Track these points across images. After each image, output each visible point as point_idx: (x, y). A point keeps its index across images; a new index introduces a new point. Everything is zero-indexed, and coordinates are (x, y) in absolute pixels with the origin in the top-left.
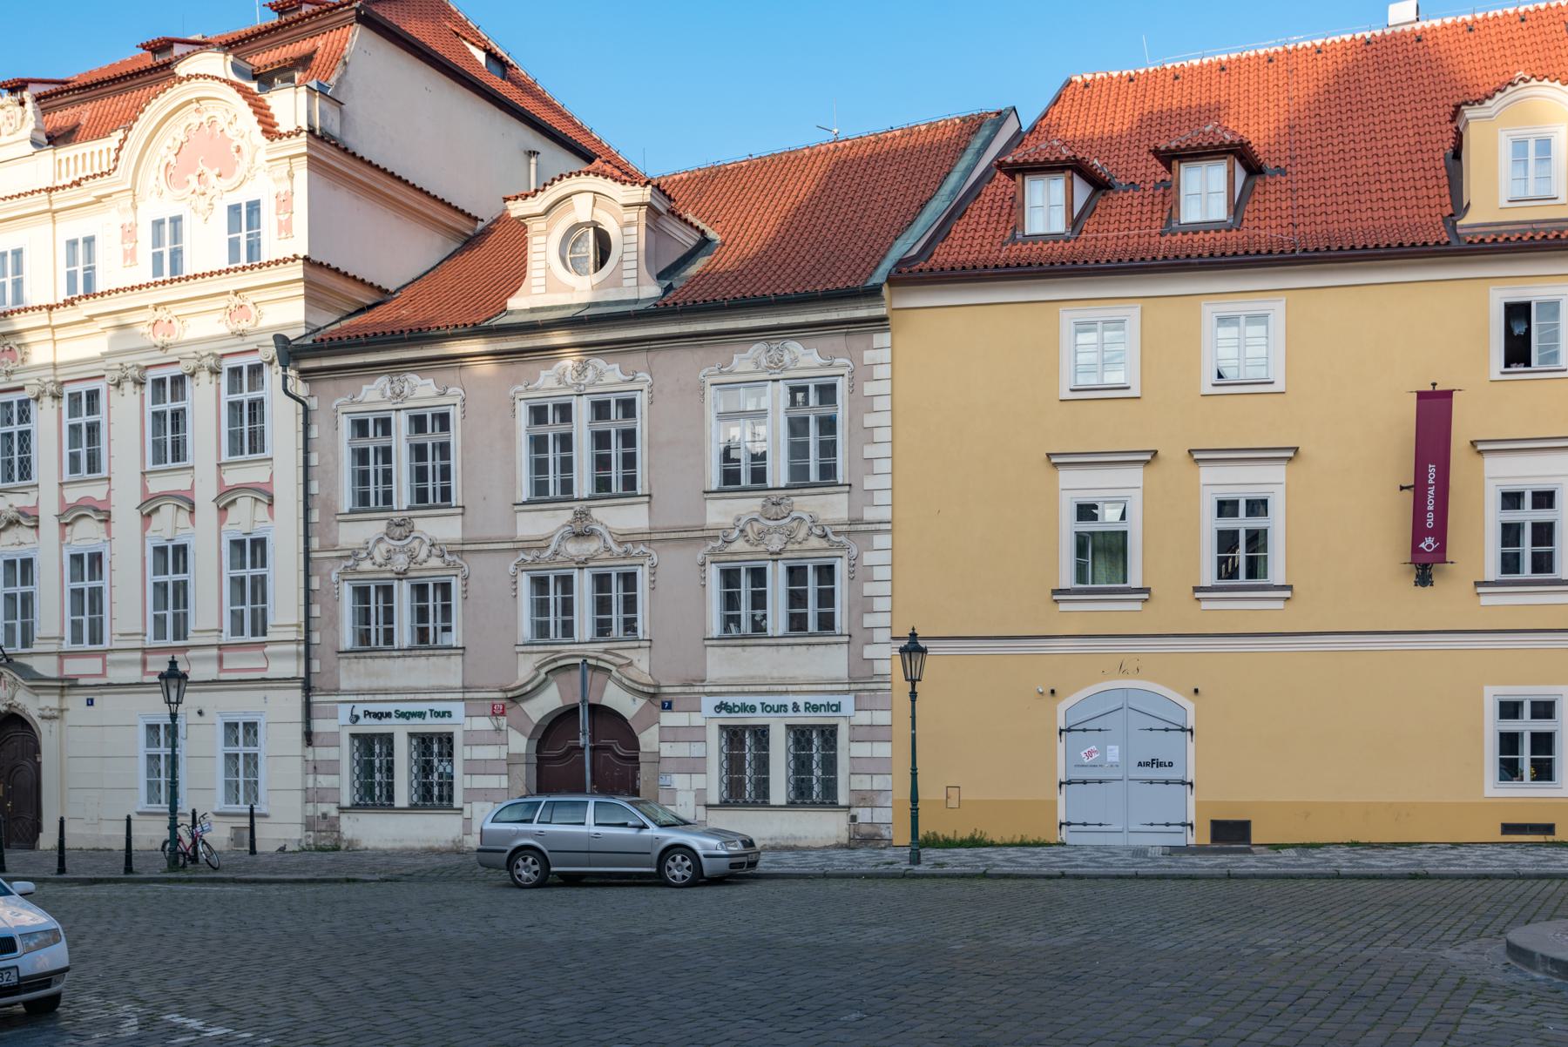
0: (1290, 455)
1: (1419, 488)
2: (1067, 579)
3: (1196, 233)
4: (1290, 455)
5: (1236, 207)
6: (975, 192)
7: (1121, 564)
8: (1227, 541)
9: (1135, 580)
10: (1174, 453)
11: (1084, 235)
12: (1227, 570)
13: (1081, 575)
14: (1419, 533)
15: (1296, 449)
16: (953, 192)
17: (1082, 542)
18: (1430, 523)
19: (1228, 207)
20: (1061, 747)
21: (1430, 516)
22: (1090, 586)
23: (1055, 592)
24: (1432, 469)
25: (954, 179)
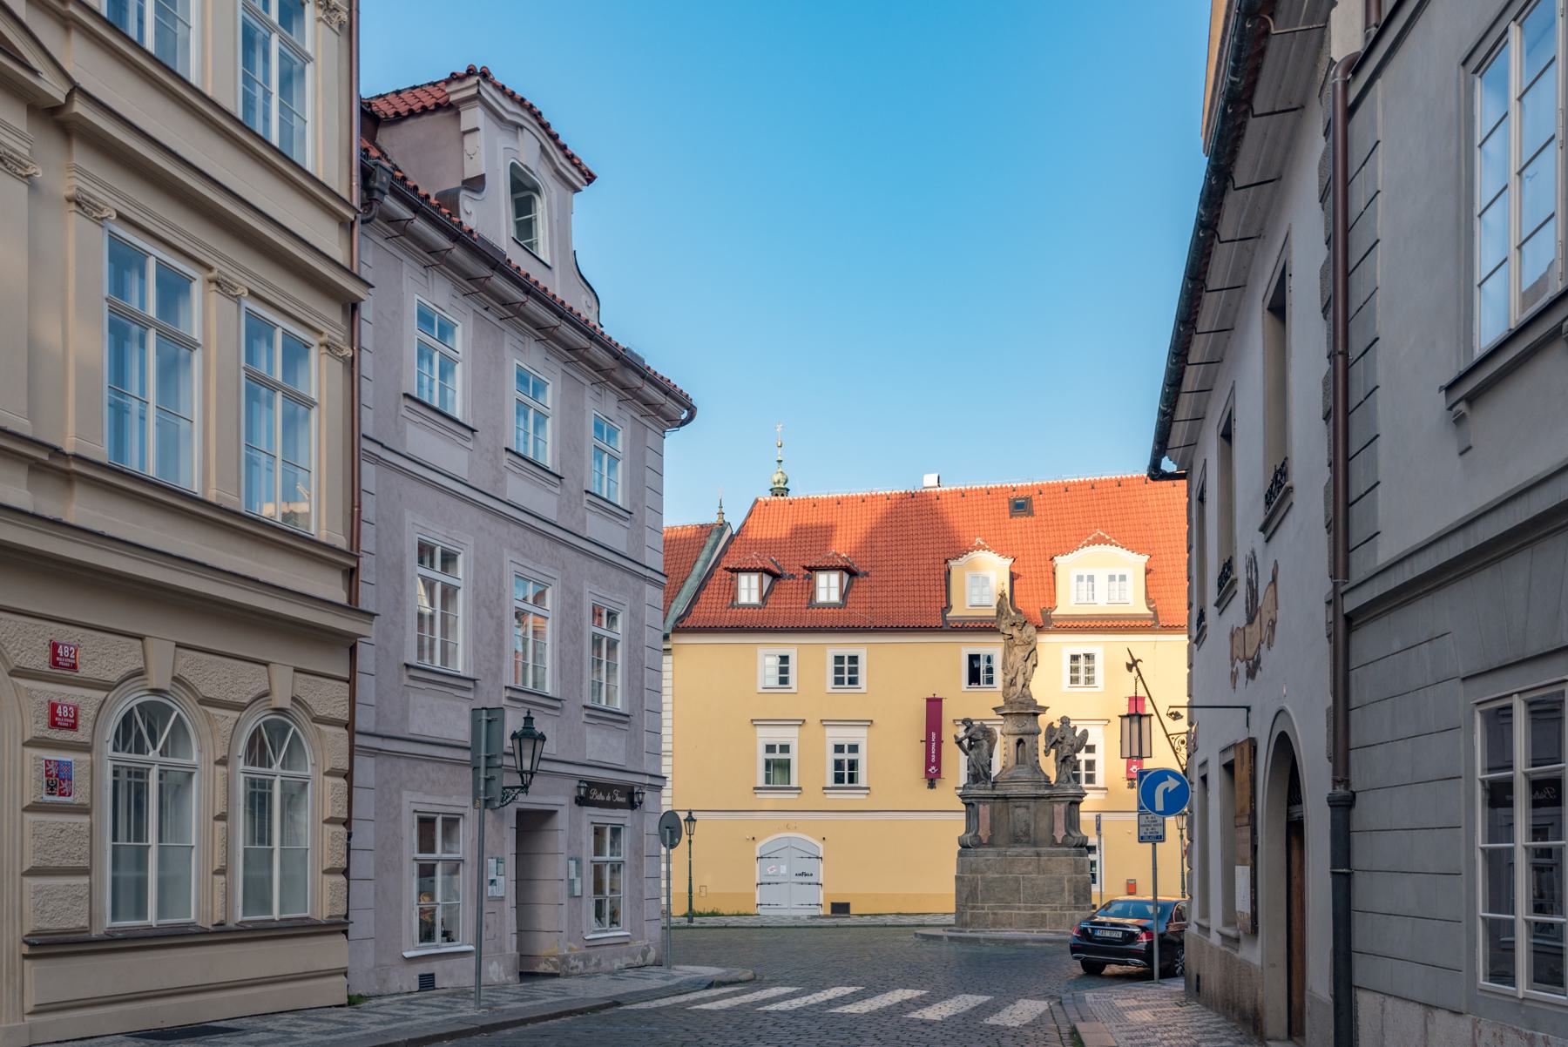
0: (870, 723)
1: (928, 741)
2: (761, 782)
3: (824, 608)
4: (870, 723)
5: (844, 596)
6: (710, 574)
7: (787, 773)
8: (838, 764)
9: (794, 783)
10: (813, 721)
11: (768, 606)
12: (839, 778)
13: (768, 781)
14: (928, 764)
15: (872, 721)
16: (700, 575)
17: (768, 763)
18: (933, 760)
19: (840, 595)
20: (757, 866)
21: (933, 756)
22: (771, 785)
23: (755, 788)
24: (934, 735)
25: (699, 565)
